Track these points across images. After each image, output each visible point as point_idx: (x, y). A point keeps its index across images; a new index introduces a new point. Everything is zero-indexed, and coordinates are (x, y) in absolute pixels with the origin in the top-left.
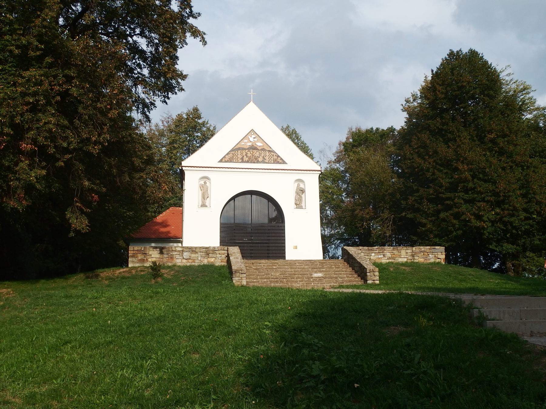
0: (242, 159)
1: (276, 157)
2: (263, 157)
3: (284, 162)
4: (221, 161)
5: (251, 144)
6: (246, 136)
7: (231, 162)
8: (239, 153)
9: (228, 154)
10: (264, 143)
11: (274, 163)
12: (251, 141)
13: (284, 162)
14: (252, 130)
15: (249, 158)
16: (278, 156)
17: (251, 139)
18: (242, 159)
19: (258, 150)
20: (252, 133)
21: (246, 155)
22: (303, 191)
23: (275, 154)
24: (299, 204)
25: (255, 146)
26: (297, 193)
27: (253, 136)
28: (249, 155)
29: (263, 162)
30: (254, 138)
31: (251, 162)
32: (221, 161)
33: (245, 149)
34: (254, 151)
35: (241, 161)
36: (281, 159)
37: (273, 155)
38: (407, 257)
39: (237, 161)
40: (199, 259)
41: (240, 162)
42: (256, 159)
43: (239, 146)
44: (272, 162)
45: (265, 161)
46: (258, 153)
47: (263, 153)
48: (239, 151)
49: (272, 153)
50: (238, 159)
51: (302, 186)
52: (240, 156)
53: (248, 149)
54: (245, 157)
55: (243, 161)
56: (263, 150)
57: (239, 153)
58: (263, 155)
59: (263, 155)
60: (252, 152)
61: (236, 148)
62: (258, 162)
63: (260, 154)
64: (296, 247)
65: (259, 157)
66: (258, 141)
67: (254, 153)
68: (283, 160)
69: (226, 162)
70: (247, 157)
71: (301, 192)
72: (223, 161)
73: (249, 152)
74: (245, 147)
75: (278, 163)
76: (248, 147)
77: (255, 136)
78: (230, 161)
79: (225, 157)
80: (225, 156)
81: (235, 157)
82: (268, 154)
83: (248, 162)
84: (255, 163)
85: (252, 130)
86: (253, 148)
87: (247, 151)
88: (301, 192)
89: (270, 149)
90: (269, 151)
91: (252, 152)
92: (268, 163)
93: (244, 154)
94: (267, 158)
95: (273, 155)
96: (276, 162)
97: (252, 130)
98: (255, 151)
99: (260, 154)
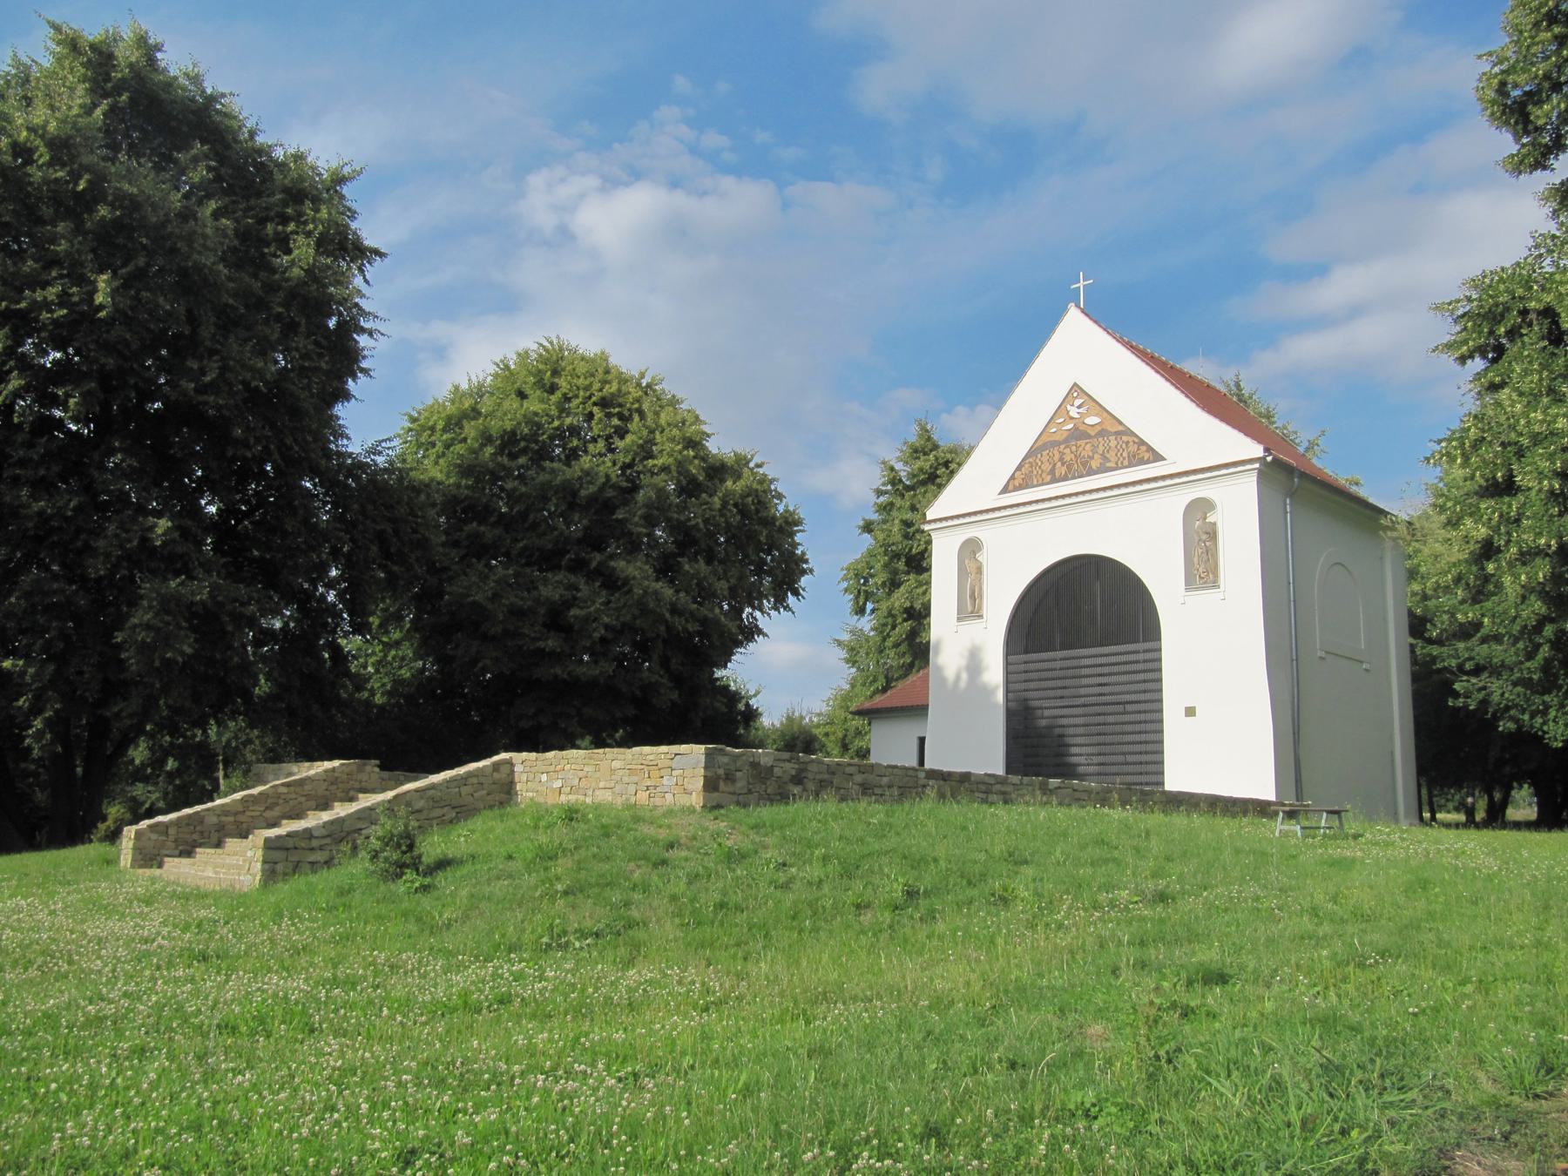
0: (1052, 472)
3: (1157, 457)
4: (1005, 490)
5: (1070, 426)
7: (1027, 486)
9: (1019, 468)
10: (1105, 414)
12: (1072, 418)
13: (1157, 457)
15: (1069, 467)
16: (1142, 442)
17: (1074, 412)
18: (1052, 472)
19: (1090, 437)
23: (1130, 439)
27: (1078, 402)
29: (1103, 469)
30: (1079, 407)
31: (1074, 478)
32: (1005, 490)
33: (1057, 443)
36: (1150, 449)
41: (1048, 483)
42: (1084, 464)
43: (1045, 438)
45: (1108, 465)
48: (1045, 453)
49: (1125, 438)
52: (1047, 467)
53: (1066, 441)
54: (1059, 464)
55: (1054, 480)
56: (1103, 433)
58: (1101, 448)
59: (1101, 448)
60: (1074, 448)
61: (1040, 443)
62: (1091, 472)
64: (1190, 712)
66: (1088, 414)
69: (1016, 489)
70: (1063, 464)
72: (1011, 487)
74: (1058, 438)
75: (1142, 462)
79: (1012, 477)
83: (1065, 478)
84: (1081, 476)
85: (1075, 384)
86: (1079, 434)
87: (1062, 447)
89: (1120, 428)
90: (1118, 433)
93: (1057, 458)
94: (1111, 455)
95: (1127, 443)
96: (1135, 461)
97: (1075, 384)
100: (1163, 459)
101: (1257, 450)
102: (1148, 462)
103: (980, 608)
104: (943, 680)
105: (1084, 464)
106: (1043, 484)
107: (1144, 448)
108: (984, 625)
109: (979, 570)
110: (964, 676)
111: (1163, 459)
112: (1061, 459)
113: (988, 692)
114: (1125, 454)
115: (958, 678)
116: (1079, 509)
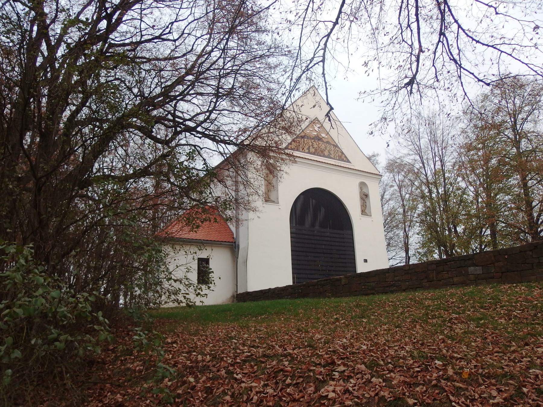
3: (348, 161)
5: (316, 134)
15: (316, 150)
16: (342, 153)
17: (316, 129)
18: (309, 149)
19: (324, 142)
22: (367, 196)
24: (365, 210)
26: (362, 198)
27: (319, 126)
28: (315, 146)
29: (329, 157)
35: (307, 151)
36: (346, 157)
46: (323, 145)
51: (364, 190)
54: (311, 147)
55: (309, 153)
56: (328, 142)
58: (328, 149)
59: (328, 149)
64: (366, 261)
65: (325, 151)
71: (364, 197)
75: (343, 160)
82: (333, 148)
84: (320, 156)
88: (364, 197)
90: (333, 145)
92: (334, 159)
94: (332, 152)
97: (316, 118)
98: (321, 143)
102: (345, 161)
105: (322, 152)
106: (304, 152)
107: (343, 156)
112: (312, 146)
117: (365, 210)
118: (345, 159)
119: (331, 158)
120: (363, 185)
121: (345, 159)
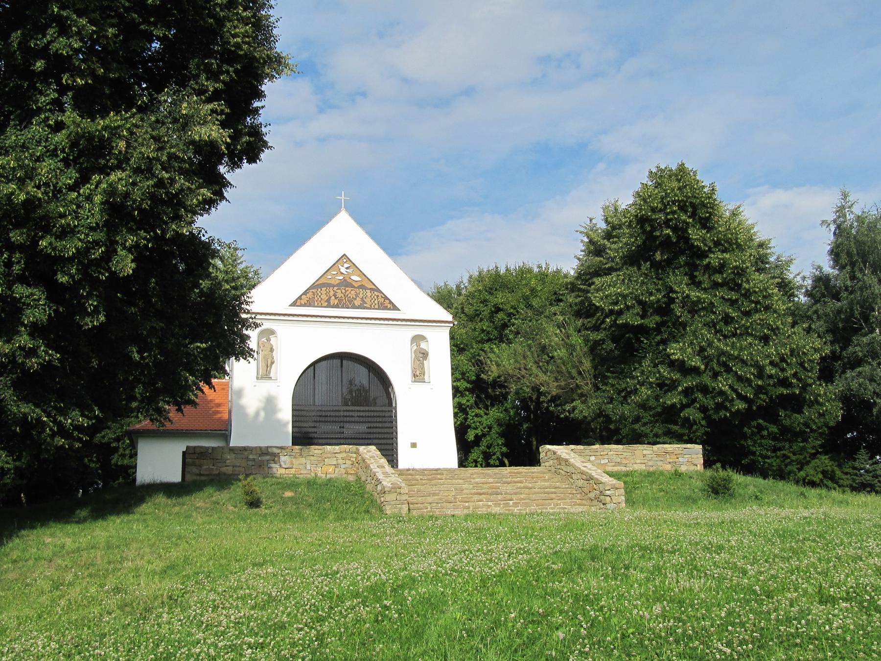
0: (328, 301)
1: (383, 299)
2: (362, 299)
3: (395, 308)
4: (294, 304)
6: (334, 264)
7: (310, 306)
8: (323, 292)
9: (305, 293)
11: (379, 309)
12: (342, 273)
13: (395, 308)
14: (344, 255)
16: (386, 298)
17: (343, 270)
18: (328, 301)
19: (354, 287)
20: (345, 261)
21: (335, 295)
22: (425, 355)
23: (380, 295)
24: (418, 375)
25: (349, 280)
27: (346, 265)
28: (339, 295)
29: (361, 307)
30: (347, 268)
31: (342, 307)
32: (294, 304)
33: (334, 286)
34: (347, 289)
36: (391, 302)
37: (378, 296)
38: (646, 461)
39: (320, 305)
40: (308, 467)
41: (325, 307)
42: (350, 302)
44: (377, 307)
46: (353, 292)
47: (362, 292)
48: (323, 289)
50: (322, 302)
51: (423, 345)
52: (324, 297)
53: (338, 285)
54: (333, 297)
55: (329, 306)
56: (362, 287)
57: (323, 292)
58: (361, 296)
59: (361, 296)
60: (343, 291)
63: (357, 295)
64: (414, 445)
65: (356, 299)
67: (348, 292)
68: (393, 304)
69: (301, 305)
70: (336, 298)
72: (298, 303)
73: (339, 291)
75: (386, 308)
76: (337, 282)
77: (348, 265)
78: (309, 304)
79: (300, 298)
80: (301, 296)
81: (316, 299)
82: (369, 294)
83: (337, 306)
84: (348, 308)
85: (345, 255)
86: (346, 283)
87: (335, 288)
89: (374, 287)
90: (371, 289)
91: (343, 291)
93: (332, 293)
94: (367, 300)
95: (378, 296)
96: (382, 307)
97: (344, 255)
98: (350, 289)
99: (357, 295)
100: (399, 310)
101: (449, 317)
102: (390, 309)
103: (270, 373)
104: (246, 415)
106: (321, 307)
107: (387, 301)
108: (278, 384)
109: (272, 350)
110: (262, 414)
111: (399, 310)
112: (335, 295)
113: (282, 424)
114: (376, 302)
115: (257, 414)
116: (359, 327)
117: (418, 375)
118: (389, 306)
119: (364, 308)
120: (418, 339)
121: (389, 306)
